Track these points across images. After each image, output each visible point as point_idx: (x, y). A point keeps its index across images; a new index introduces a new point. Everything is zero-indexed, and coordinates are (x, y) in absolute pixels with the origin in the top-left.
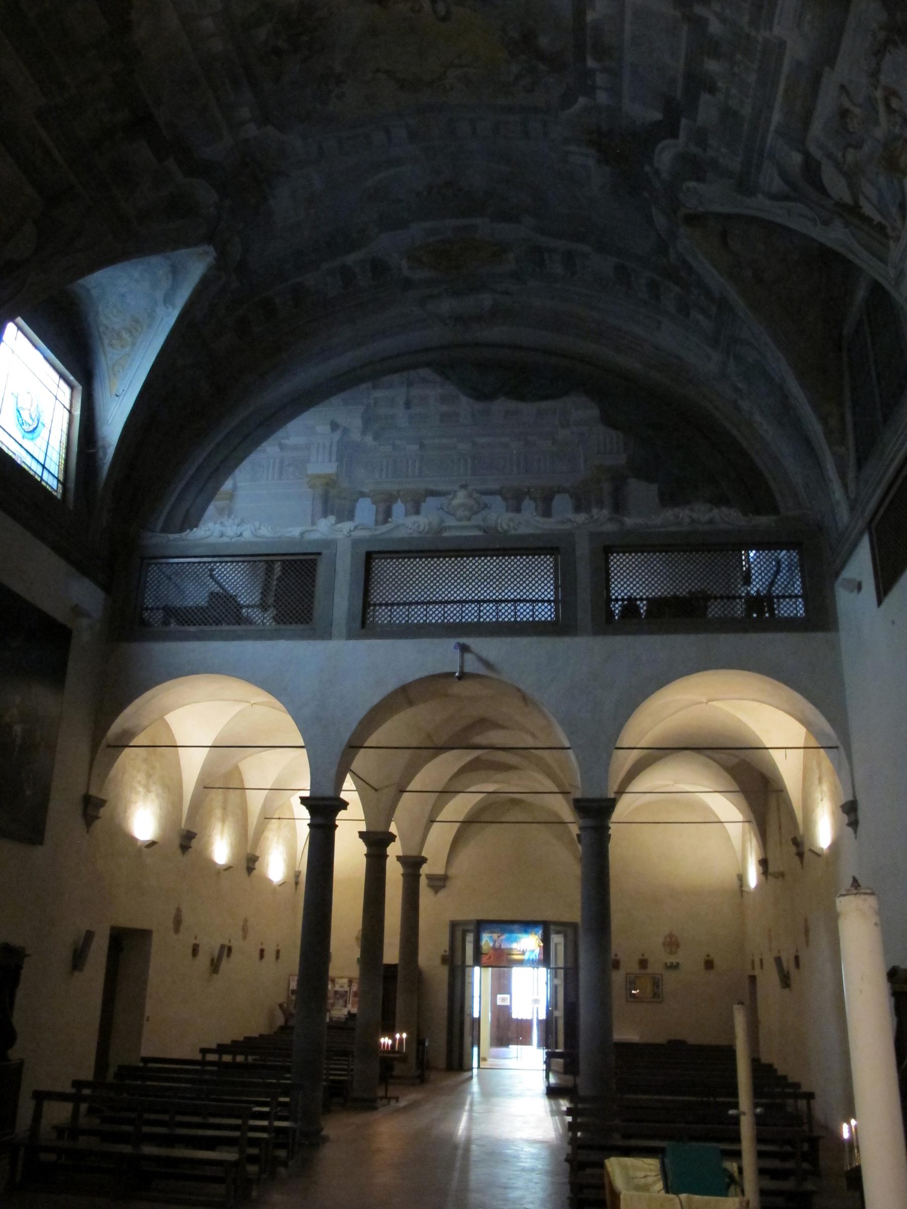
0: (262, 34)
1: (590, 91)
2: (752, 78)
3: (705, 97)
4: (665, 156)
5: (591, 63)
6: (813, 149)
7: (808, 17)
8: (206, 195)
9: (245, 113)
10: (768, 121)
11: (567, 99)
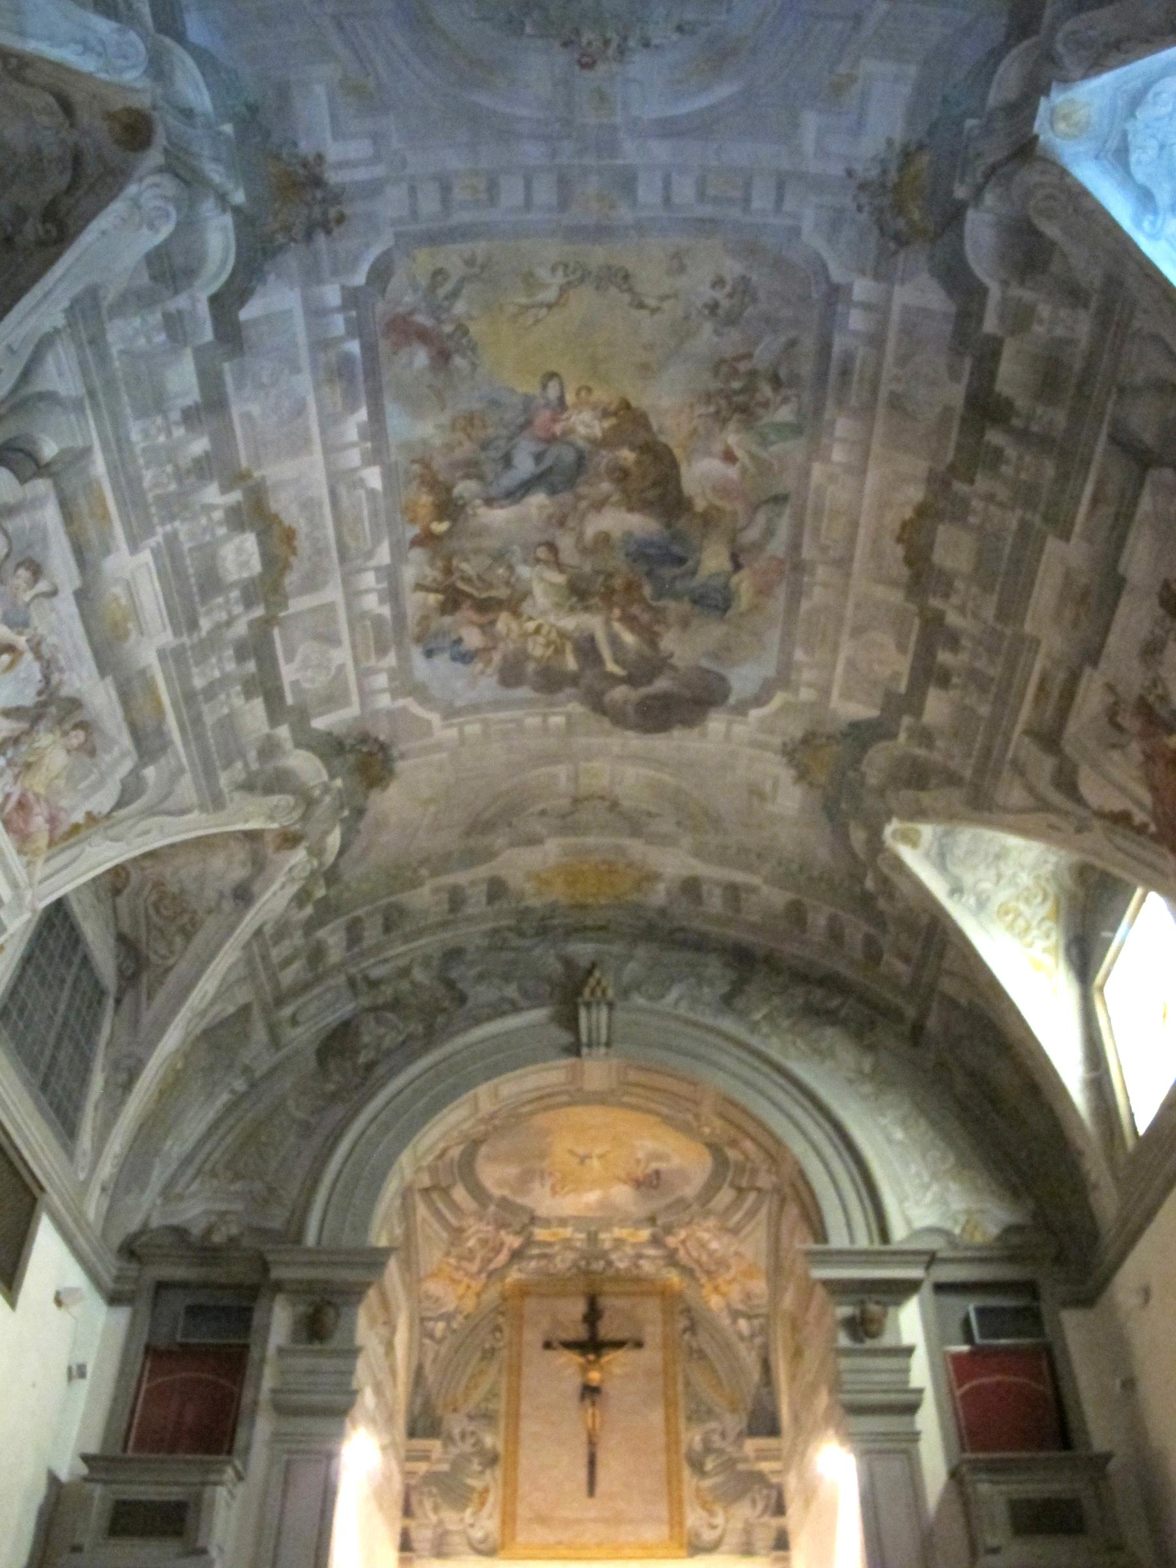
0: (785, 414)
1: (352, 298)
2: (148, 476)
3: (194, 397)
4: (219, 241)
5: (354, 347)
6: (42, 486)
7: (123, 601)
8: (980, 234)
9: (857, 321)
10: (105, 448)
11: (381, 273)
